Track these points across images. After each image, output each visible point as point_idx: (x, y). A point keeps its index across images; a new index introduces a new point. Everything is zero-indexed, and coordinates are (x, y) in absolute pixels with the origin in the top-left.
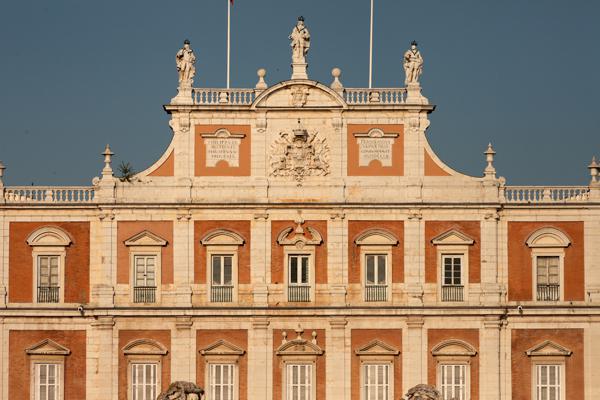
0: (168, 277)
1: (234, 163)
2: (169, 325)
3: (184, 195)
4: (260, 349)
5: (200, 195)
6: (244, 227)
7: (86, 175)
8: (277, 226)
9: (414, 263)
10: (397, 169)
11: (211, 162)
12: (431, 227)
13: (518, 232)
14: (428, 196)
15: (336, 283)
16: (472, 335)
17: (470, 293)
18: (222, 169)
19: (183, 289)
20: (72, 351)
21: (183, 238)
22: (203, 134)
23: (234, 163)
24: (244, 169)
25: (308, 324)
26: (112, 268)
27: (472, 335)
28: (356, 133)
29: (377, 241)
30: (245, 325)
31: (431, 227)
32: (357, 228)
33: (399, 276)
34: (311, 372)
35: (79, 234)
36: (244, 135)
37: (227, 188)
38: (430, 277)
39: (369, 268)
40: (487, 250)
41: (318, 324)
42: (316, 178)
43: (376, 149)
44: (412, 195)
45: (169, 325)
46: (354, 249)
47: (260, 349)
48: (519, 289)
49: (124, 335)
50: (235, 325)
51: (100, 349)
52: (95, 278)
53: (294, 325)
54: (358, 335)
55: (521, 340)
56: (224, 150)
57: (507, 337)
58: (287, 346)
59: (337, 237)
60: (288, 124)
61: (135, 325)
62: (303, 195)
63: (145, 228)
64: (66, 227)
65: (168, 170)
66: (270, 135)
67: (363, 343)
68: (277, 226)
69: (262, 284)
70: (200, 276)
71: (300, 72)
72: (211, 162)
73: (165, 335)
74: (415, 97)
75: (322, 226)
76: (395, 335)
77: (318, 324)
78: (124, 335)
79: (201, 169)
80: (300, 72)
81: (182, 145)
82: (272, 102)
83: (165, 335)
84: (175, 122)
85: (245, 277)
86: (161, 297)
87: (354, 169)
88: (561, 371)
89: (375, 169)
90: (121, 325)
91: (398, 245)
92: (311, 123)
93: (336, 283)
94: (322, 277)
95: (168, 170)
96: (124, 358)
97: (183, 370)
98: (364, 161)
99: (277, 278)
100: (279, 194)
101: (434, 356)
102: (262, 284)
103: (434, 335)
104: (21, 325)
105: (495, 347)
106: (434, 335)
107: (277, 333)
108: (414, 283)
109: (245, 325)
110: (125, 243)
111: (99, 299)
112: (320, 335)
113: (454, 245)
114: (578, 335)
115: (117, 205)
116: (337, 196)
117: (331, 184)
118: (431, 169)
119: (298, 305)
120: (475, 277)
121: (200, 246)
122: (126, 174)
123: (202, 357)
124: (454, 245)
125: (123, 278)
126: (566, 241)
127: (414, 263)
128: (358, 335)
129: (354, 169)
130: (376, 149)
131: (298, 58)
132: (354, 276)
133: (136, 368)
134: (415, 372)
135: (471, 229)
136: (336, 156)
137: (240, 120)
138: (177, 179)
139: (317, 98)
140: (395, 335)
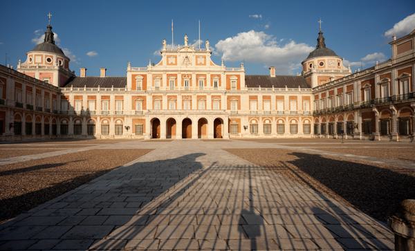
0: (162, 85)
1: (174, 63)
2: (162, 94)
4: (179, 99)
5: (167, 69)
6: (176, 75)
7: (146, 65)
8: (182, 75)
10: (205, 64)
11: (170, 62)
12: (212, 75)
13: (228, 77)
14: (212, 69)
15: (194, 87)
16: (220, 96)
17: (219, 88)
18: (172, 64)
19: (164, 88)
20: (144, 100)
21: (165, 77)
22: (168, 57)
23: (174, 63)
24: (176, 64)
25: (188, 94)
26: (151, 83)
27: (220, 96)
28: (197, 57)
29: (202, 78)
30: (177, 94)
31: (212, 75)
32: (197, 75)
33: (205, 85)
34: (189, 103)
35: (145, 76)
38: (212, 85)
39: (201, 84)
40: (222, 80)
41: (190, 94)
43: (201, 60)
44: (208, 69)
45: (162, 94)
46: (197, 79)
47: (179, 99)
48: (228, 88)
49: (153, 96)
50: (175, 94)
51: (149, 99)
52: (148, 85)
53: (186, 94)
54: (198, 96)
55: (229, 98)
56: (172, 60)
57: (226, 97)
58: (185, 98)
60: (184, 55)
61: (155, 94)
62: (187, 69)
63: (157, 76)
64: (142, 75)
65: (161, 64)
66: (181, 57)
67: (199, 98)
68: (182, 75)
70: (168, 85)
71: (186, 45)
72: (170, 62)
73: (161, 96)
74: (208, 50)
75: (191, 75)
76: (205, 97)
77: (190, 94)
78: (153, 96)
79: (168, 64)
80: (186, 45)
81: (164, 59)
82: (181, 51)
83: (161, 96)
84: (163, 54)
85: (176, 85)
86: (161, 89)
87: (197, 64)
88: (236, 104)
89: (201, 64)
90: (153, 94)
92: (189, 55)
93: (194, 87)
94: (191, 85)
95: (161, 64)
96: (153, 101)
98: (199, 62)
99: (183, 85)
100: (182, 69)
101: (212, 101)
102: (180, 87)
103: (212, 97)
104: (134, 95)
105: (224, 99)
106: (212, 97)
107: (183, 96)
108: (209, 87)
109: (177, 94)
110: (154, 79)
111: (149, 89)
112: (191, 97)
113: (216, 79)
114: (239, 97)
116: (194, 69)
117: (193, 67)
118: (211, 64)
119: (186, 91)
120: (220, 85)
121: (168, 79)
122: (153, 65)
125: (153, 85)
126: (237, 78)
128: (198, 96)
129: (197, 64)
130: (201, 60)
131: (186, 42)
132: (197, 85)
133: (155, 103)
135: (219, 76)
136: (193, 61)
137: (175, 54)
138: (163, 66)
139: (189, 50)
140: (205, 97)
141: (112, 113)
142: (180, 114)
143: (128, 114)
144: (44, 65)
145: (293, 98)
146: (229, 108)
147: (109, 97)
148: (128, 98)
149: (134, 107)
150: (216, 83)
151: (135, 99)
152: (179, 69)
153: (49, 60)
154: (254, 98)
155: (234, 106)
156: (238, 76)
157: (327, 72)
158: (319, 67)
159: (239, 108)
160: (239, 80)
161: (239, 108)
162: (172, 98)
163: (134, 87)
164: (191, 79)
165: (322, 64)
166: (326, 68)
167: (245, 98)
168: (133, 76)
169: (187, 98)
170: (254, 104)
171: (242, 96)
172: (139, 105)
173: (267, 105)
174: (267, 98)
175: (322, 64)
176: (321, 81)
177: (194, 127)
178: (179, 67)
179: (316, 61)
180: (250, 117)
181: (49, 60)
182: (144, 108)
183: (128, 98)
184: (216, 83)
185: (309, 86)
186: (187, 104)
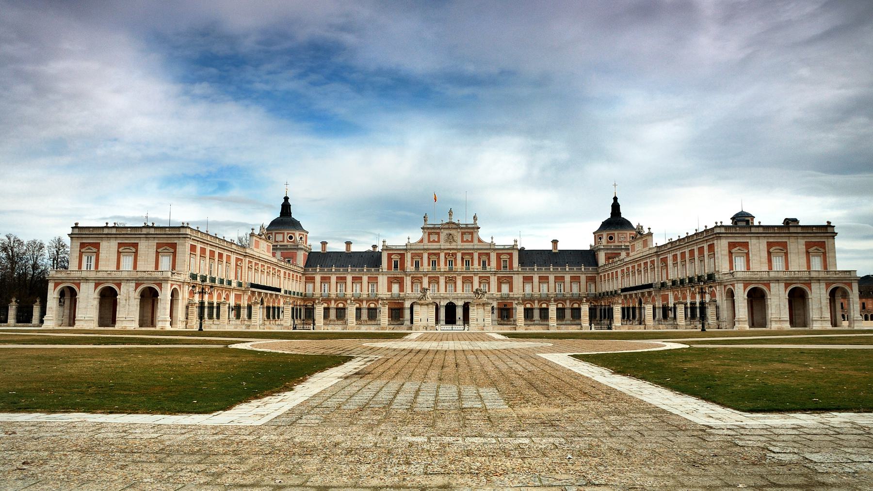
3: (426, 247)
4: (442, 281)
8: (446, 254)
9: (476, 262)
17: (488, 267)
18: (434, 241)
21: (425, 256)
24: (439, 241)
28: (463, 234)
29: (467, 257)
36: (438, 234)
37: (435, 246)
38: (479, 265)
42: (454, 244)
44: (476, 247)
46: (462, 259)
47: (442, 281)
51: (408, 281)
55: (499, 278)
59: (459, 256)
69: (443, 266)
70: (429, 265)
89: (467, 241)
91: (472, 259)
92: (452, 232)
94: (456, 265)
96: (412, 283)
97: (425, 285)
102: (443, 266)
105: (493, 280)
106: (480, 278)
108: (476, 266)
115: (411, 249)
116: (459, 247)
117: (459, 244)
119: (451, 270)
120: (489, 265)
121: (429, 258)
123: (429, 283)
124: (484, 258)
127: (476, 262)
129: (463, 241)
132: (463, 265)
134: (476, 286)
135: (488, 255)
141: (365, 296)
142: (444, 298)
143: (384, 297)
144: (285, 243)
145: (575, 279)
146: (499, 290)
147: (361, 278)
148: (383, 280)
149: (390, 289)
150: (484, 263)
151: (390, 282)
152: (442, 247)
153: (291, 238)
154: (528, 279)
155: (505, 288)
156: (511, 255)
157: (619, 248)
158: (608, 242)
159: (511, 290)
160: (511, 259)
161: (511, 290)
162: (434, 280)
163: (389, 268)
164: (455, 259)
165: (611, 238)
166: (617, 244)
167: (518, 280)
168: (389, 255)
169: (451, 280)
170: (528, 288)
171: (515, 277)
172: (395, 288)
173: (544, 287)
174: (543, 279)
175: (611, 238)
176: (609, 258)
177: (459, 313)
178: (443, 244)
179: (605, 235)
180: (524, 300)
181: (291, 238)
182: (402, 289)
183: (383, 280)
184: (484, 263)
185: (597, 265)
186: (450, 287)
